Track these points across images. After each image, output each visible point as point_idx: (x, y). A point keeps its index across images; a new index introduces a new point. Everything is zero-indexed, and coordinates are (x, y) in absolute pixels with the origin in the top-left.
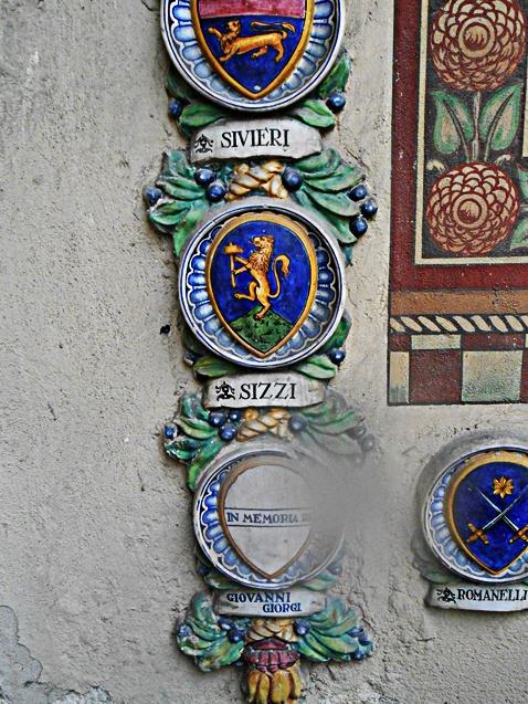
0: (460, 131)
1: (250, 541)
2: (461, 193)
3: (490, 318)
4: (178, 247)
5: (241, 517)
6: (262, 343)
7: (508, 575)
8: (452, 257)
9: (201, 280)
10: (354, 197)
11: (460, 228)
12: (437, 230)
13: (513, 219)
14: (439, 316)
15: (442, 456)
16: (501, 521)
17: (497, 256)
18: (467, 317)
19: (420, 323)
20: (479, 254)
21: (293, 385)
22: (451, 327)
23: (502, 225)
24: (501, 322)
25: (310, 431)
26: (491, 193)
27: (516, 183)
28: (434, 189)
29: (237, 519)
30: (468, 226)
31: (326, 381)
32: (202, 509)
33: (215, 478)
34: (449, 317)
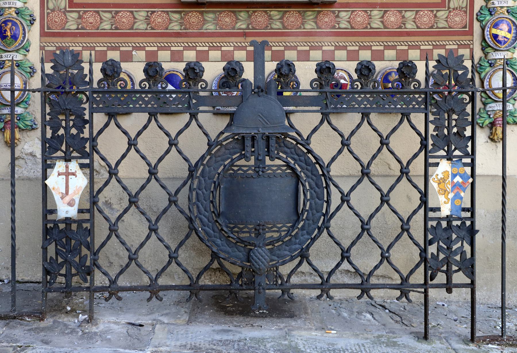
0: (54, 5)
6: (9, 45)
12: (50, 24)
18: (57, 43)
20: (59, 30)
27: (65, 15)
34: (53, 43)
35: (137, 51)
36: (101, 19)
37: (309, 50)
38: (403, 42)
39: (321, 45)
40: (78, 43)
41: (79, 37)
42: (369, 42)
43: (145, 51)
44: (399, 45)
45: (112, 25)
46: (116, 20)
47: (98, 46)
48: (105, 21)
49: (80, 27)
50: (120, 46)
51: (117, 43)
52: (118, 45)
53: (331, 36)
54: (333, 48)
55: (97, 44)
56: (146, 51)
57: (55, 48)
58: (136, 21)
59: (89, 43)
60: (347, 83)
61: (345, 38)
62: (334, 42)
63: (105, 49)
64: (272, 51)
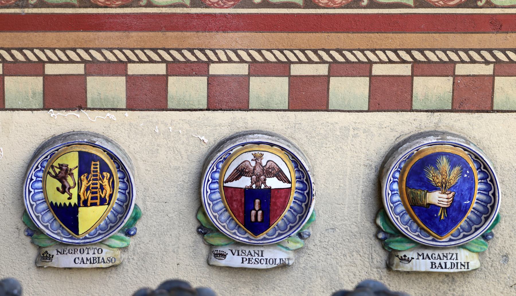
37: (166, 76)
38: (478, 51)
39: (204, 59)
42: (362, 51)
44: (462, 62)
53: (237, 29)
54: (243, 69)
60: (287, 185)
61: (284, 35)
62: (247, 51)
64: (46, 77)
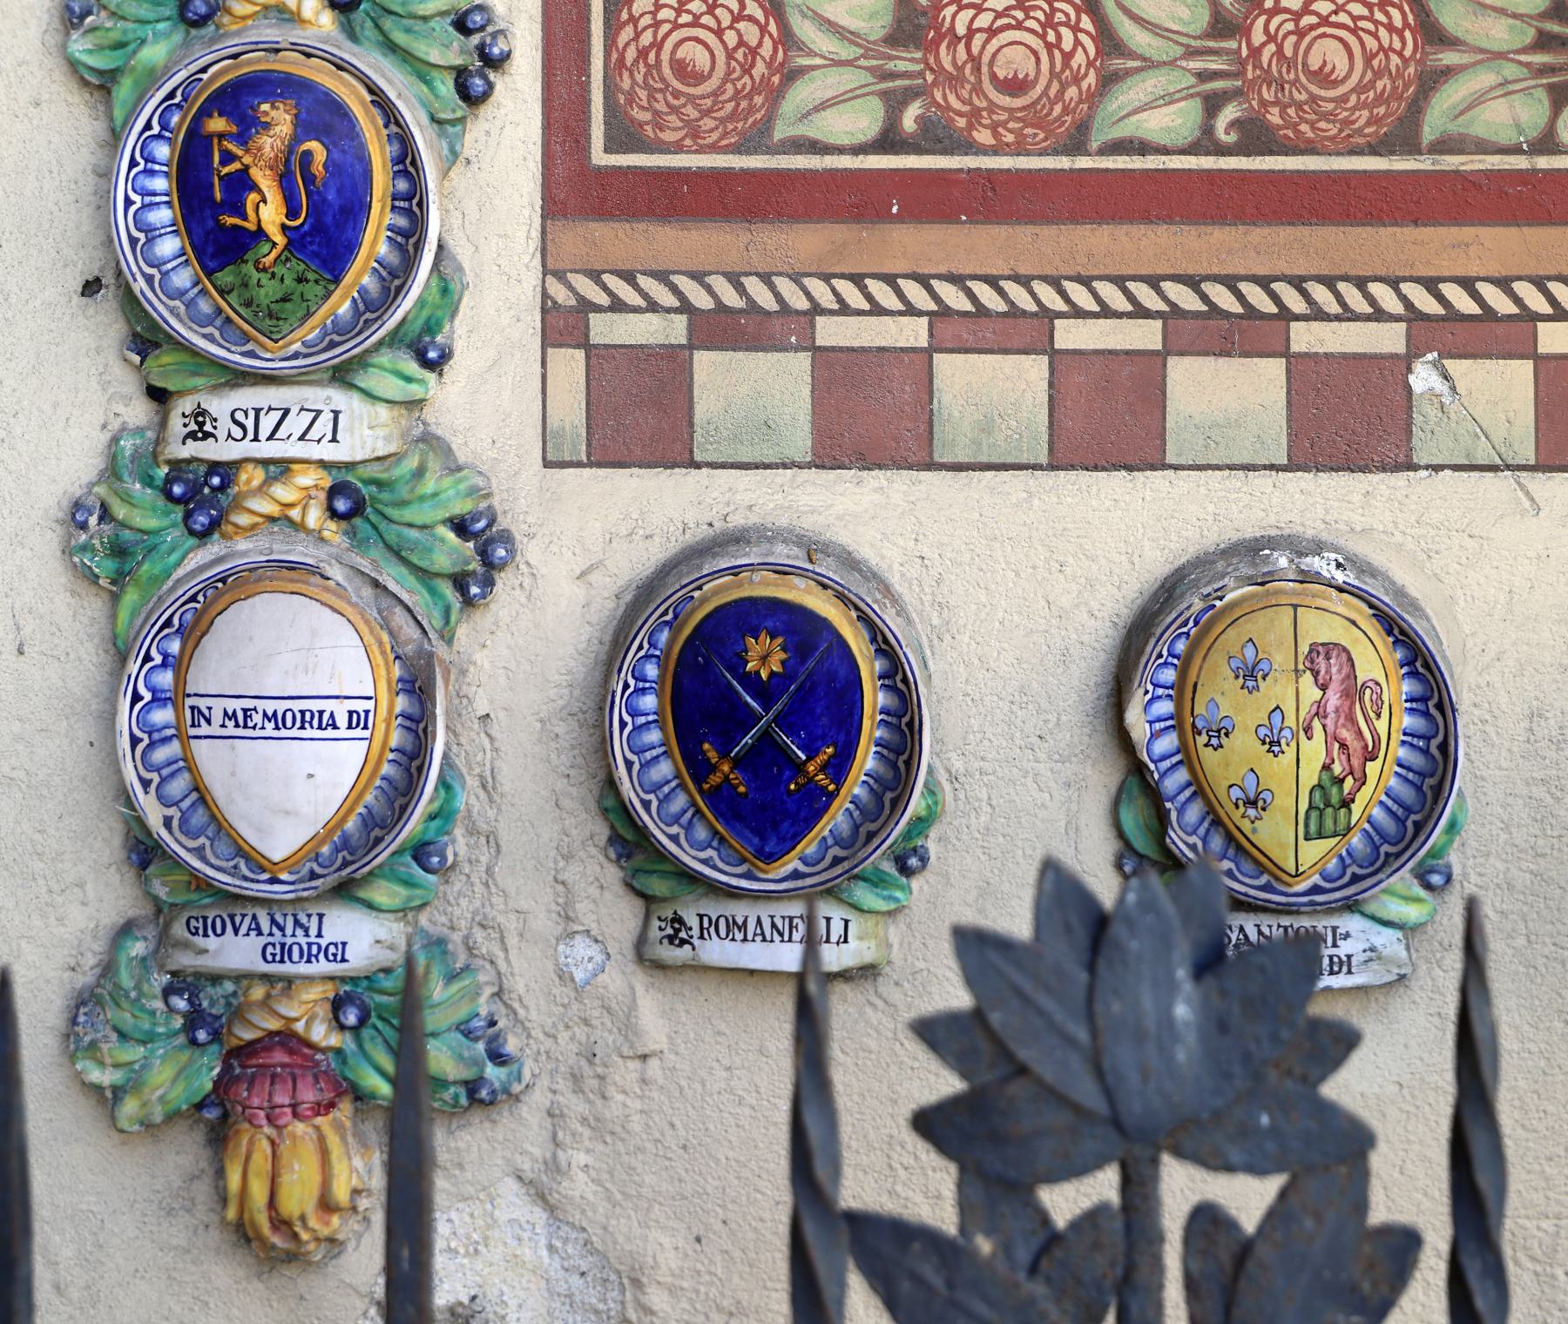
1: (233, 774)
2: (676, 26)
3: (743, 279)
4: (119, 114)
5: (217, 717)
7: (796, 875)
8: (661, 152)
9: (160, 184)
10: (462, 25)
11: (677, 94)
12: (631, 98)
13: (776, 79)
14: (644, 273)
15: (647, 590)
16: (766, 736)
17: (748, 152)
18: (698, 277)
19: (605, 288)
20: (714, 148)
21: (336, 413)
22: (668, 300)
23: (755, 90)
24: (786, 295)
25: (373, 517)
26: (731, 27)
28: (625, 16)
29: (209, 722)
30: (691, 90)
31: (414, 405)
32: (136, 697)
33: (168, 623)
34: (662, 276)
35: (1453, 366)
36: (1109, 41)
40: (890, 280)
41: (899, 218)
43: (1528, 365)
45: (1212, 104)
46: (1256, 52)
47: (1078, 313)
48: (1150, 64)
49: (909, 122)
50: (1286, 315)
51: (1264, 282)
52: (1267, 306)
55: (1069, 286)
56: (1540, 360)
57: (681, 321)
58: (1449, 58)
59: (992, 281)
63: (1147, 335)
